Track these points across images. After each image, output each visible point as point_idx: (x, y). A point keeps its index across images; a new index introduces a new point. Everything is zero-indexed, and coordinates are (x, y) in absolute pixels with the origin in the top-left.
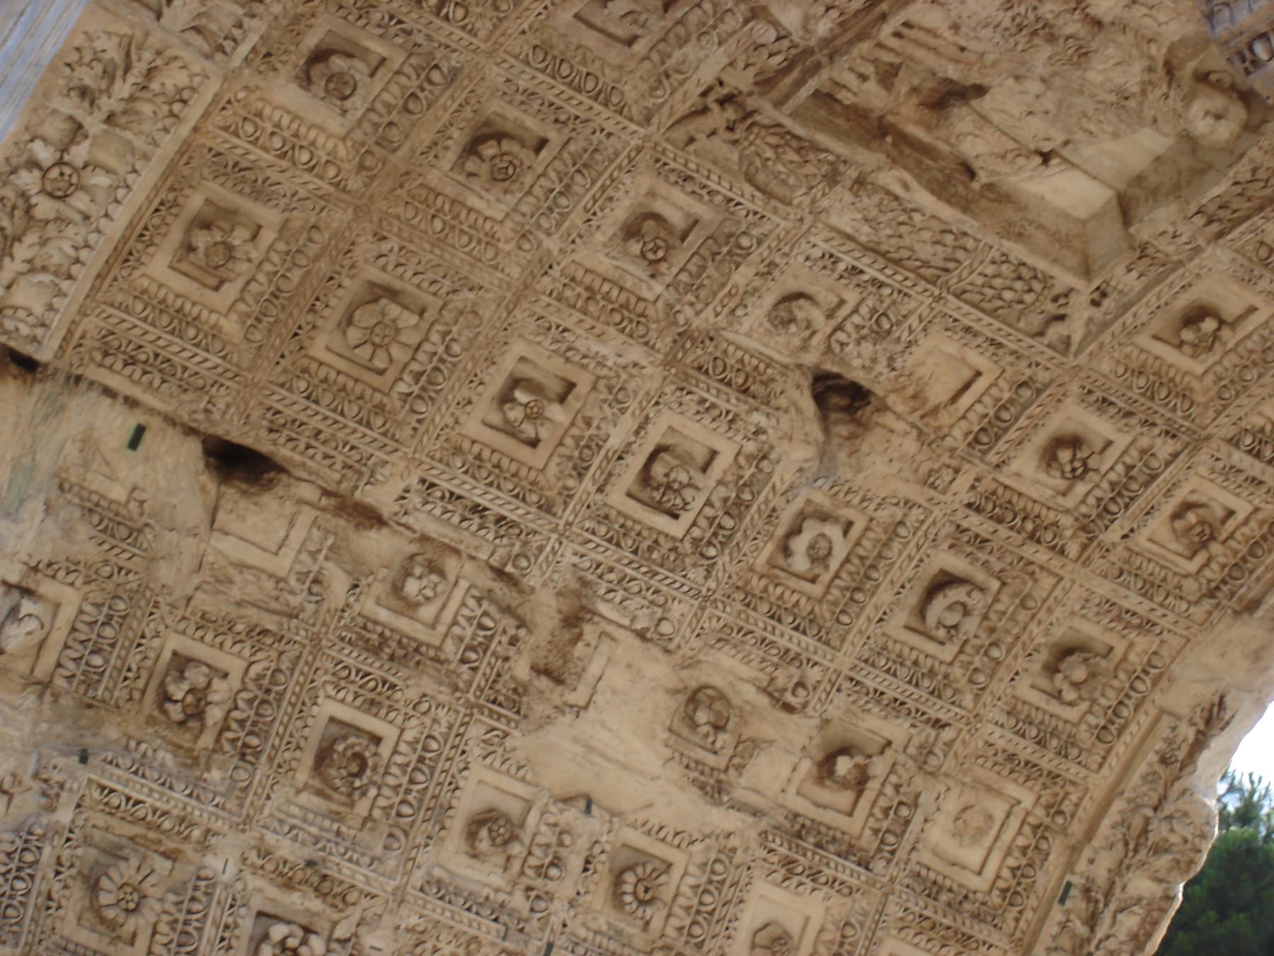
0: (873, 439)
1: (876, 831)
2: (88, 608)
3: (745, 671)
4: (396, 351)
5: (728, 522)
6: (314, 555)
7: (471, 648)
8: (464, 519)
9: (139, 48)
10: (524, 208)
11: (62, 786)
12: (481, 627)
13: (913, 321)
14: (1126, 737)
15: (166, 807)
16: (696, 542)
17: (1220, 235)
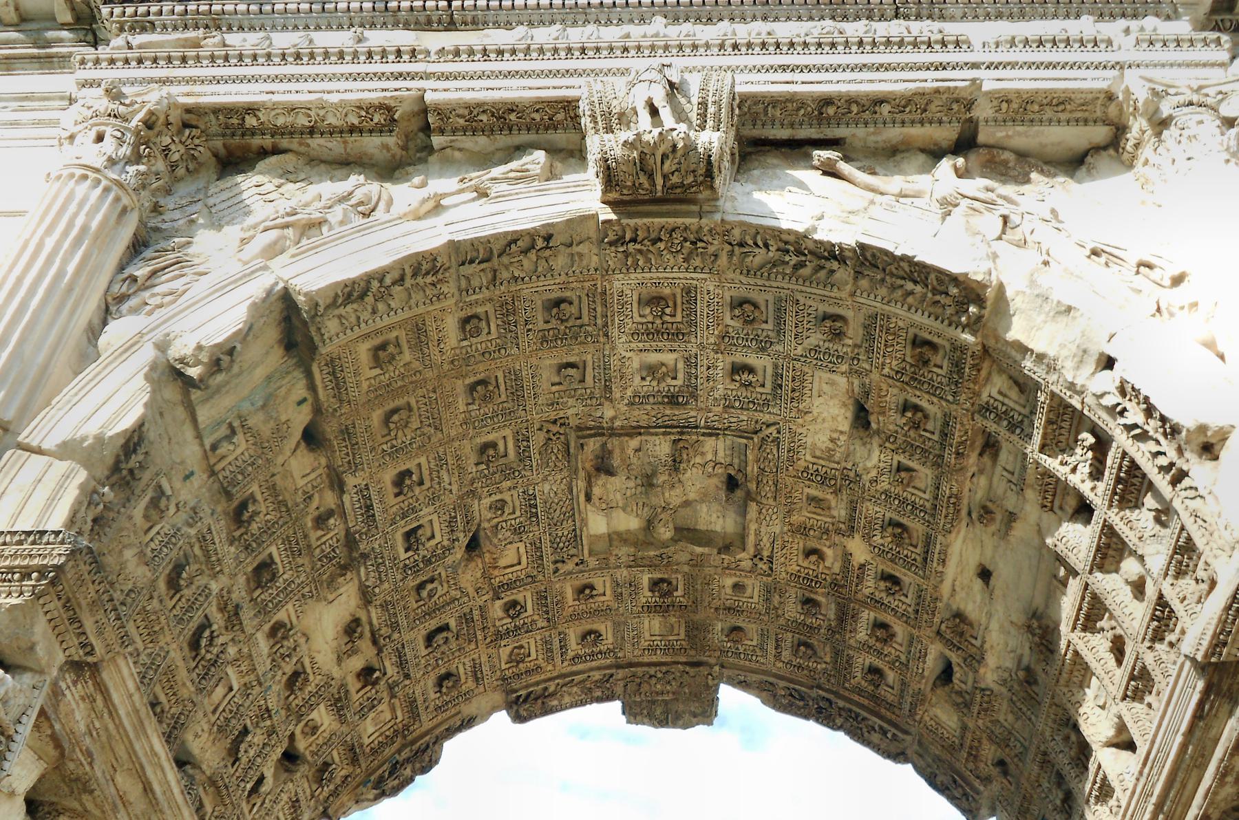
0: (472, 565)
1: (361, 704)
2: (246, 454)
3: (375, 621)
4: (400, 433)
5: (421, 565)
6: (314, 487)
7: (326, 557)
8: (360, 508)
9: (445, 270)
10: (473, 414)
11: (201, 519)
12: (333, 550)
13: (531, 534)
14: (444, 714)
15: (219, 552)
16: (406, 565)
17: (630, 567)
